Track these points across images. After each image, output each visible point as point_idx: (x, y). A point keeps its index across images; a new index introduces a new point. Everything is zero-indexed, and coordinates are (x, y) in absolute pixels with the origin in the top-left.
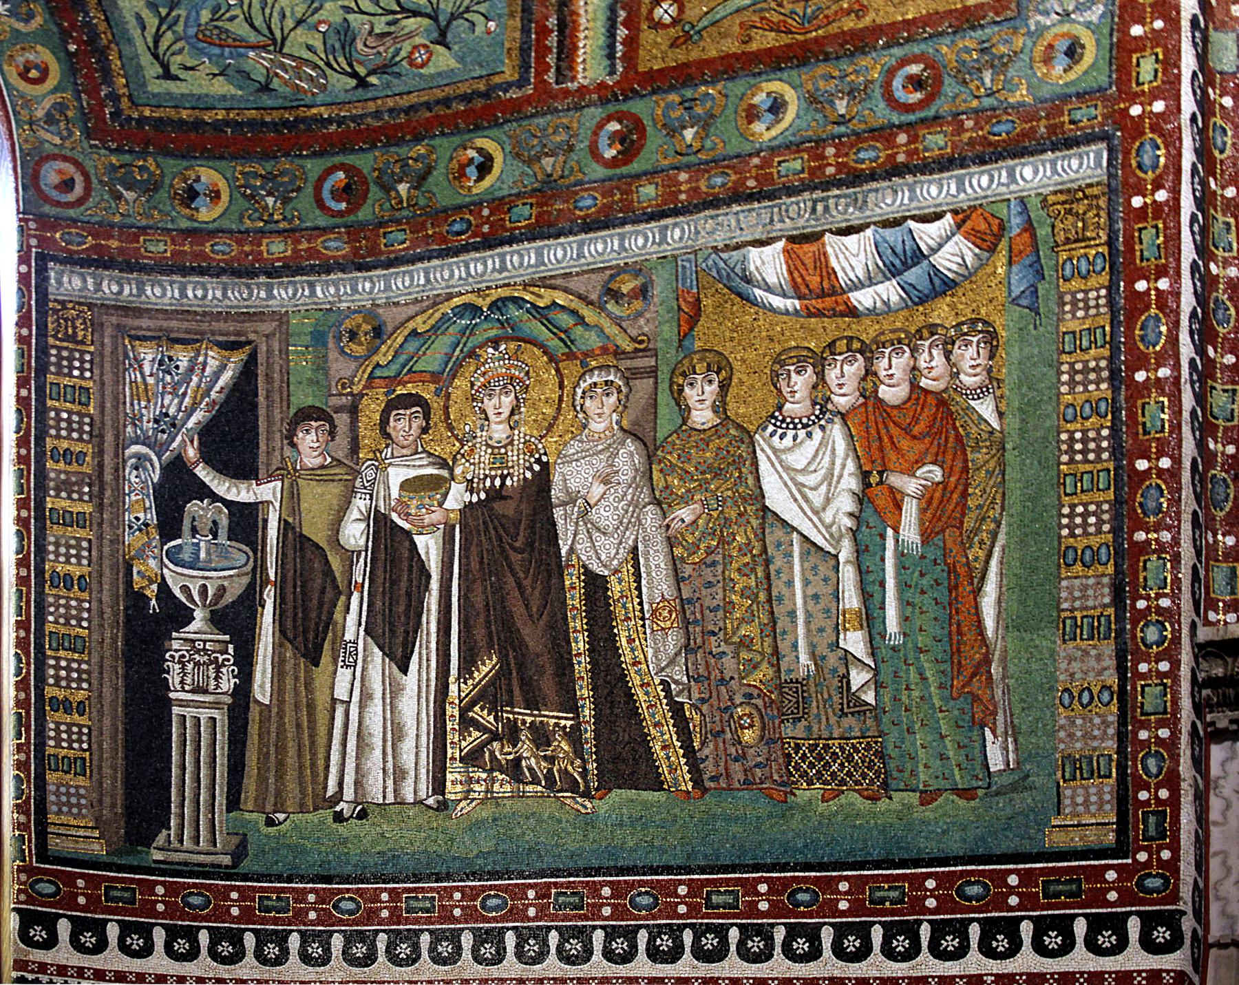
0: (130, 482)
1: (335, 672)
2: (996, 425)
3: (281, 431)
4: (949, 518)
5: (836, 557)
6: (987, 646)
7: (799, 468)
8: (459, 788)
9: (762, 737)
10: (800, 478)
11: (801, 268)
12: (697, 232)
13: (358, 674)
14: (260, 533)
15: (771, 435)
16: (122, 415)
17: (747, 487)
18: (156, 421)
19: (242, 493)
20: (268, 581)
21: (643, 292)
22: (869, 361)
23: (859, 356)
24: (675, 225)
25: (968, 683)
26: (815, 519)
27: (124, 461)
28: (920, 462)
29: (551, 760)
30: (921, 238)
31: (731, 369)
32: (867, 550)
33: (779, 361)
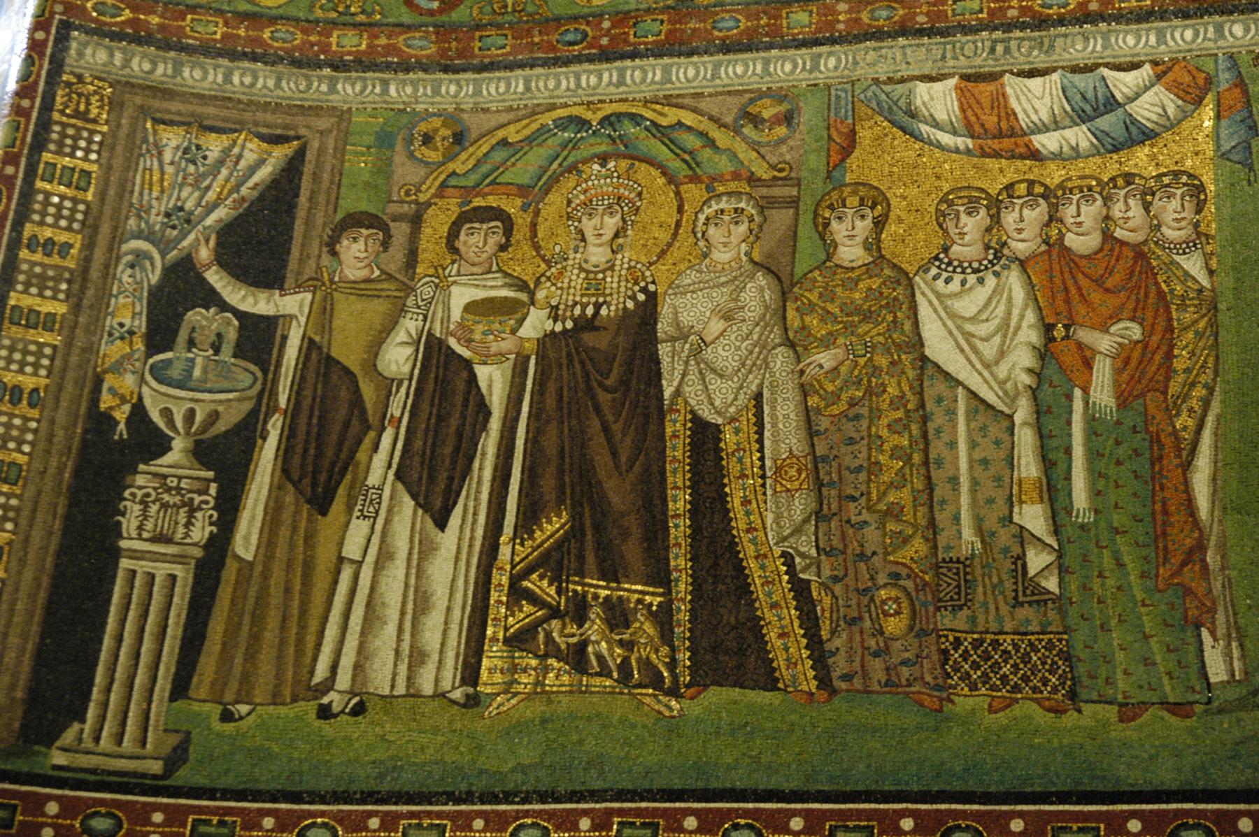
0: (121, 281)
3: (321, 237)
5: (1010, 417)
7: (967, 315)
10: (969, 327)
15: (935, 278)
17: (903, 333)
20: (276, 409)
21: (788, 119)
26: (986, 373)
31: (889, 205)
32: (1049, 411)
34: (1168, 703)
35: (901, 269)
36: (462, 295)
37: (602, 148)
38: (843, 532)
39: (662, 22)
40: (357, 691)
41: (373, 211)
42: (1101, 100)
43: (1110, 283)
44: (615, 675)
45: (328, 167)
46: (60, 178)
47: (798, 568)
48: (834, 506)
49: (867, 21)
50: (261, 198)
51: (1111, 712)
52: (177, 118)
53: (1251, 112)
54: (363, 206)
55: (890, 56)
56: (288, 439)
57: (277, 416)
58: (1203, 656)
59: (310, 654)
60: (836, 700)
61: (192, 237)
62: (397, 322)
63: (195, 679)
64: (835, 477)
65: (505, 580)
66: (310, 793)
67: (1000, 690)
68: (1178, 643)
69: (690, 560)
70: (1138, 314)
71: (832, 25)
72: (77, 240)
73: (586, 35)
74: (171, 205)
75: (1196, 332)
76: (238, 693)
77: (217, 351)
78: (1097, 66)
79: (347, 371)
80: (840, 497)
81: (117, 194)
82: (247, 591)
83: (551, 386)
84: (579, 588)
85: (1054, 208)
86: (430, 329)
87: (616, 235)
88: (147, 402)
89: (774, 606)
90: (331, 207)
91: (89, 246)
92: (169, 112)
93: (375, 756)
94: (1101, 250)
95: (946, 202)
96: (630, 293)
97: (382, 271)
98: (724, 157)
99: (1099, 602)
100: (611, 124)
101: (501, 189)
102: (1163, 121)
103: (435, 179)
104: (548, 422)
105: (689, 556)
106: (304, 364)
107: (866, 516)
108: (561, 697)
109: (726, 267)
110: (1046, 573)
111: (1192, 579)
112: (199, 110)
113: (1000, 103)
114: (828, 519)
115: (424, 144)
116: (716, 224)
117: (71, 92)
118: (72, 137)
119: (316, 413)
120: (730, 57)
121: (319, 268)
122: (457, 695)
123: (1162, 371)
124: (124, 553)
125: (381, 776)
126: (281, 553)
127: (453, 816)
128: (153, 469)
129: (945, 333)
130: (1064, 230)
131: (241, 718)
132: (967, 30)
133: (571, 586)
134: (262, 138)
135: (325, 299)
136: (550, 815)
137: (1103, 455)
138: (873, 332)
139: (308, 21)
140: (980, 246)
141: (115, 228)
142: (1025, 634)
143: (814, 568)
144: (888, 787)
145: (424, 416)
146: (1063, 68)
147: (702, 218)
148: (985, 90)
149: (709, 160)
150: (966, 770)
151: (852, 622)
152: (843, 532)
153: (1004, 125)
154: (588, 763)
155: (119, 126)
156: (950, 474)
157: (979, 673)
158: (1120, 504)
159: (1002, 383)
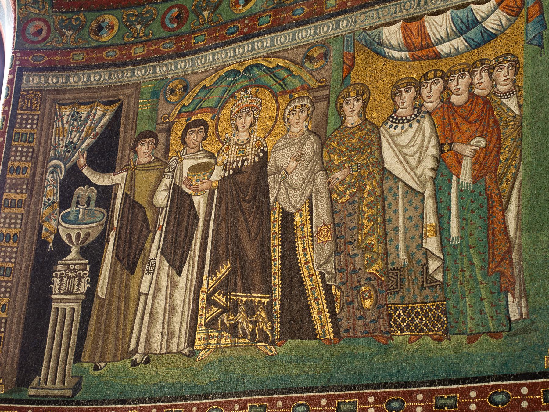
1: (142, 277)
2: (517, 112)
4: (489, 167)
6: (510, 242)
8: (202, 342)
9: (375, 304)
11: (410, 35)
12: (356, 22)
13: (155, 277)
16: (49, 145)
18: (66, 146)
19: (103, 180)
20: (113, 228)
22: (446, 82)
23: (440, 80)
24: (344, 19)
25: (499, 265)
27: (47, 169)
28: (472, 137)
29: (255, 323)
30: (477, 13)
33: (396, 86)
36: (188, 163)
37: (244, 84)
38: (346, 260)
47: (327, 279)
51: (464, 339)
56: (118, 241)
57: (113, 231)
62: (161, 181)
64: (343, 233)
65: (205, 297)
67: (414, 332)
69: (281, 280)
79: (141, 206)
80: (345, 243)
86: (175, 182)
87: (251, 126)
95: (396, 87)
97: (155, 158)
98: (297, 80)
100: (249, 71)
101: (203, 110)
103: (176, 110)
104: (222, 221)
105: (280, 278)
109: (297, 134)
110: (437, 271)
114: (340, 254)
115: (171, 94)
116: (293, 114)
119: (129, 228)
130: (450, 93)
142: (426, 303)
143: (333, 279)
145: (172, 223)
147: (287, 111)
149: (291, 81)
152: (346, 260)
158: (473, 233)
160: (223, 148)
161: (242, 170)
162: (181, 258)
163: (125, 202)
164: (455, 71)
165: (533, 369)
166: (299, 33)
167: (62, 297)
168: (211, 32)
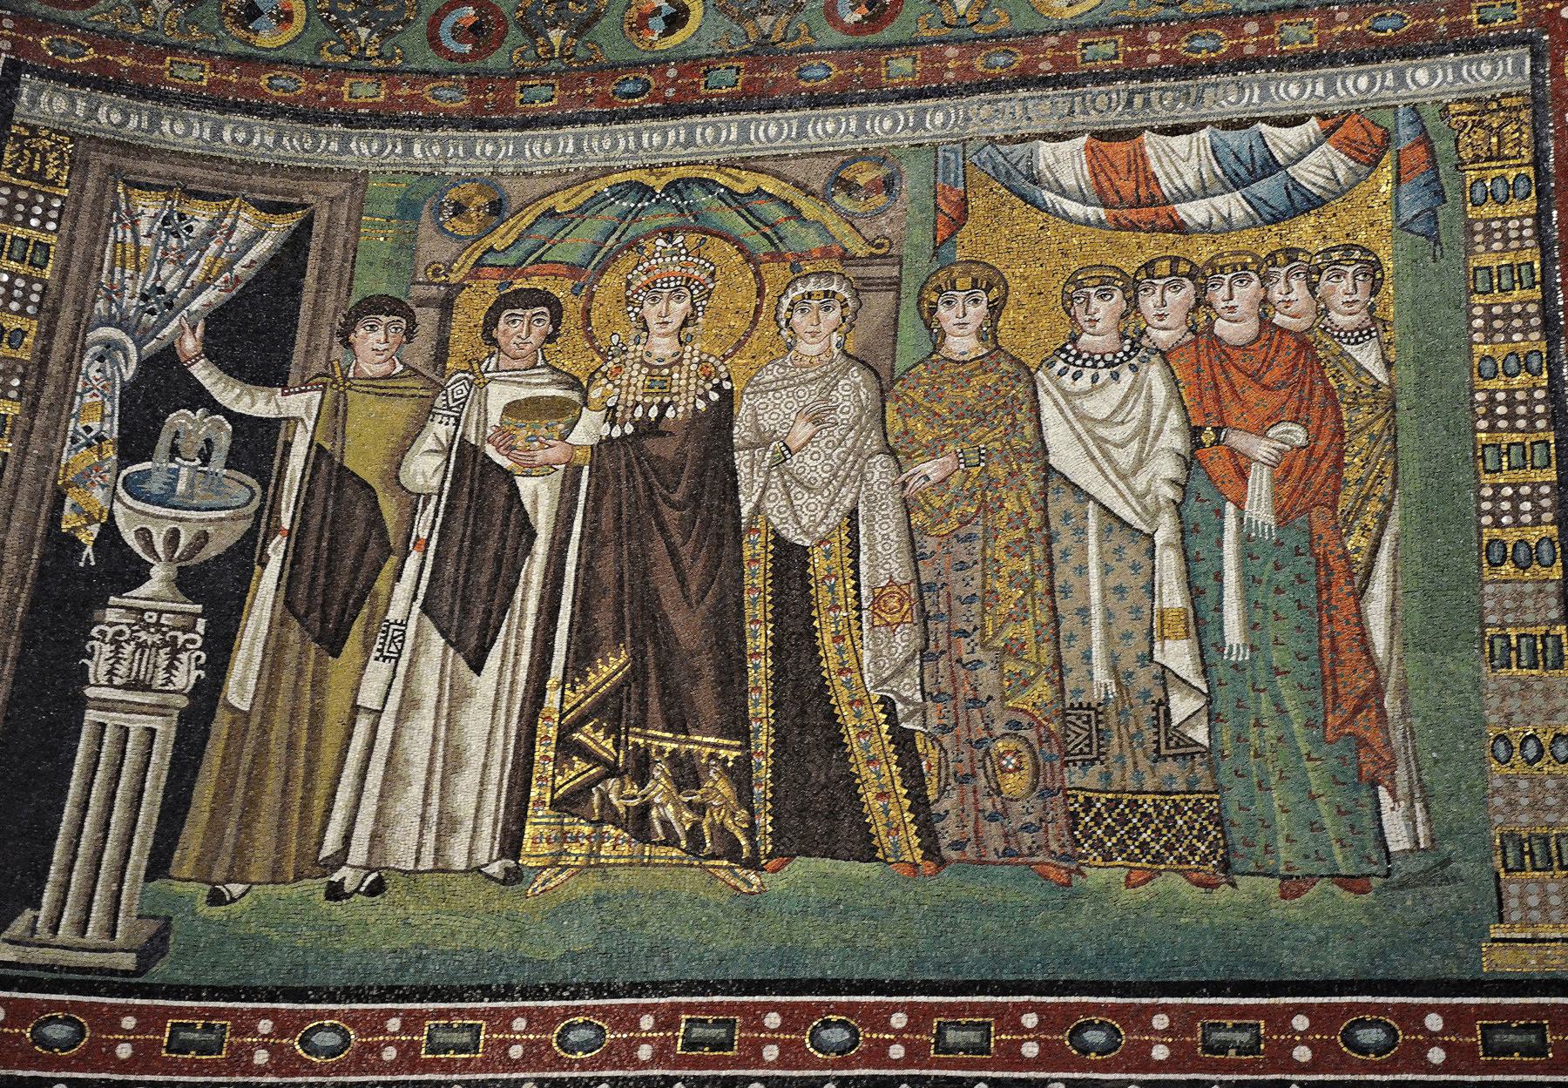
1: (364, 667)
5: (1151, 537)
10: (1101, 431)
14: (277, 462)
17: (1023, 438)
20: (278, 529)
21: (888, 185)
26: (1121, 485)
31: (1007, 287)
32: (1196, 530)
34: (1339, 876)
35: (1021, 364)
36: (501, 393)
37: (667, 221)
39: (738, 70)
40: (374, 865)
41: (393, 293)
42: (1258, 162)
43: (1268, 379)
44: (683, 843)
45: (340, 242)
46: (10, 252)
47: (900, 716)
48: (943, 643)
49: (982, 70)
50: (258, 278)
51: (1271, 886)
52: (156, 181)
53: (1437, 174)
54: (382, 289)
55: (1008, 110)
56: (292, 565)
57: (278, 538)
58: (1380, 820)
59: (317, 821)
60: (945, 872)
61: (175, 323)
63: (177, 854)
64: (944, 610)
65: (552, 732)
66: (316, 989)
68: (1350, 804)
70: (1301, 415)
71: (939, 73)
72: (32, 327)
73: (649, 86)
74: (148, 286)
75: (1371, 436)
76: (231, 867)
77: (206, 460)
78: (1254, 121)
79: (365, 485)
80: (949, 631)
81: (82, 271)
82: (242, 747)
83: (608, 503)
84: (641, 741)
85: (1202, 290)
86: (463, 435)
87: (685, 324)
88: (120, 522)
89: (870, 761)
90: (344, 290)
91: (49, 334)
92: (145, 174)
93: (394, 944)
94: (1258, 338)
96: (700, 392)
99: (1257, 756)
100: (679, 192)
101: (548, 268)
102: (1331, 186)
103: (468, 257)
104: (604, 545)
106: (312, 476)
107: (979, 654)
108: (619, 871)
111: (1367, 729)
112: (181, 171)
113: (1138, 163)
115: (455, 214)
117: (23, 147)
118: (24, 202)
119: (327, 535)
120: (820, 111)
121: (329, 362)
122: (495, 869)
123: (1331, 482)
124: (90, 703)
125: (402, 968)
126: (283, 701)
127: (489, 1015)
128: (126, 602)
129: (1072, 437)
131: (233, 900)
132: (1100, 78)
133: (631, 739)
134: (261, 206)
135: (337, 400)
136: (606, 1012)
137: (1260, 582)
138: (989, 438)
139: (313, 66)
140: (1114, 336)
141: (80, 313)
144: (1007, 976)
145: (456, 538)
146: (1213, 124)
147: (786, 303)
148: (1121, 149)
149: (795, 233)
150: (1099, 955)
151: (964, 779)
153: (1143, 192)
154: (651, 949)
155: (83, 188)
156: (1080, 604)
157: (1114, 840)
158: (1281, 640)
159: (1140, 497)
160: (604, 369)
161: (662, 427)
162: (484, 626)
163: (316, 467)
164: (1222, 268)
165: (1453, 971)
166: (815, 123)
167: (119, 695)
168: (568, 79)
